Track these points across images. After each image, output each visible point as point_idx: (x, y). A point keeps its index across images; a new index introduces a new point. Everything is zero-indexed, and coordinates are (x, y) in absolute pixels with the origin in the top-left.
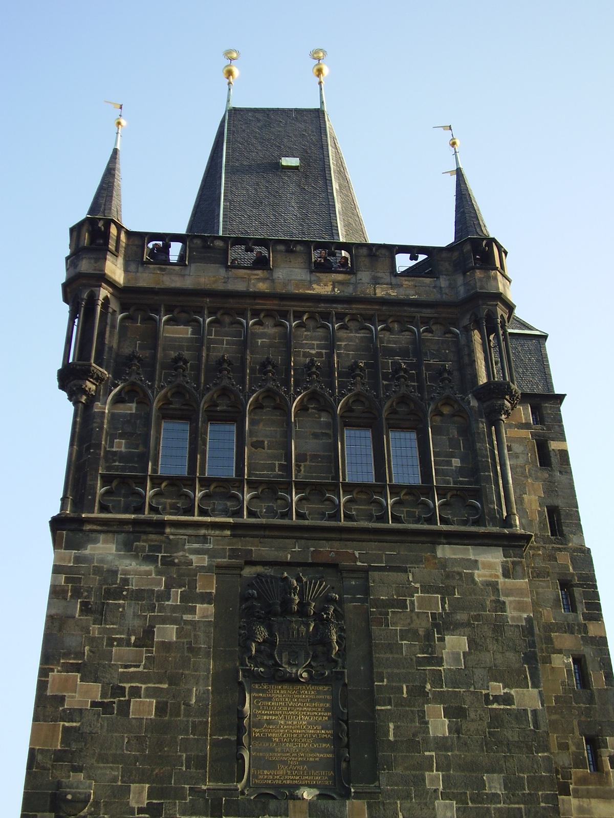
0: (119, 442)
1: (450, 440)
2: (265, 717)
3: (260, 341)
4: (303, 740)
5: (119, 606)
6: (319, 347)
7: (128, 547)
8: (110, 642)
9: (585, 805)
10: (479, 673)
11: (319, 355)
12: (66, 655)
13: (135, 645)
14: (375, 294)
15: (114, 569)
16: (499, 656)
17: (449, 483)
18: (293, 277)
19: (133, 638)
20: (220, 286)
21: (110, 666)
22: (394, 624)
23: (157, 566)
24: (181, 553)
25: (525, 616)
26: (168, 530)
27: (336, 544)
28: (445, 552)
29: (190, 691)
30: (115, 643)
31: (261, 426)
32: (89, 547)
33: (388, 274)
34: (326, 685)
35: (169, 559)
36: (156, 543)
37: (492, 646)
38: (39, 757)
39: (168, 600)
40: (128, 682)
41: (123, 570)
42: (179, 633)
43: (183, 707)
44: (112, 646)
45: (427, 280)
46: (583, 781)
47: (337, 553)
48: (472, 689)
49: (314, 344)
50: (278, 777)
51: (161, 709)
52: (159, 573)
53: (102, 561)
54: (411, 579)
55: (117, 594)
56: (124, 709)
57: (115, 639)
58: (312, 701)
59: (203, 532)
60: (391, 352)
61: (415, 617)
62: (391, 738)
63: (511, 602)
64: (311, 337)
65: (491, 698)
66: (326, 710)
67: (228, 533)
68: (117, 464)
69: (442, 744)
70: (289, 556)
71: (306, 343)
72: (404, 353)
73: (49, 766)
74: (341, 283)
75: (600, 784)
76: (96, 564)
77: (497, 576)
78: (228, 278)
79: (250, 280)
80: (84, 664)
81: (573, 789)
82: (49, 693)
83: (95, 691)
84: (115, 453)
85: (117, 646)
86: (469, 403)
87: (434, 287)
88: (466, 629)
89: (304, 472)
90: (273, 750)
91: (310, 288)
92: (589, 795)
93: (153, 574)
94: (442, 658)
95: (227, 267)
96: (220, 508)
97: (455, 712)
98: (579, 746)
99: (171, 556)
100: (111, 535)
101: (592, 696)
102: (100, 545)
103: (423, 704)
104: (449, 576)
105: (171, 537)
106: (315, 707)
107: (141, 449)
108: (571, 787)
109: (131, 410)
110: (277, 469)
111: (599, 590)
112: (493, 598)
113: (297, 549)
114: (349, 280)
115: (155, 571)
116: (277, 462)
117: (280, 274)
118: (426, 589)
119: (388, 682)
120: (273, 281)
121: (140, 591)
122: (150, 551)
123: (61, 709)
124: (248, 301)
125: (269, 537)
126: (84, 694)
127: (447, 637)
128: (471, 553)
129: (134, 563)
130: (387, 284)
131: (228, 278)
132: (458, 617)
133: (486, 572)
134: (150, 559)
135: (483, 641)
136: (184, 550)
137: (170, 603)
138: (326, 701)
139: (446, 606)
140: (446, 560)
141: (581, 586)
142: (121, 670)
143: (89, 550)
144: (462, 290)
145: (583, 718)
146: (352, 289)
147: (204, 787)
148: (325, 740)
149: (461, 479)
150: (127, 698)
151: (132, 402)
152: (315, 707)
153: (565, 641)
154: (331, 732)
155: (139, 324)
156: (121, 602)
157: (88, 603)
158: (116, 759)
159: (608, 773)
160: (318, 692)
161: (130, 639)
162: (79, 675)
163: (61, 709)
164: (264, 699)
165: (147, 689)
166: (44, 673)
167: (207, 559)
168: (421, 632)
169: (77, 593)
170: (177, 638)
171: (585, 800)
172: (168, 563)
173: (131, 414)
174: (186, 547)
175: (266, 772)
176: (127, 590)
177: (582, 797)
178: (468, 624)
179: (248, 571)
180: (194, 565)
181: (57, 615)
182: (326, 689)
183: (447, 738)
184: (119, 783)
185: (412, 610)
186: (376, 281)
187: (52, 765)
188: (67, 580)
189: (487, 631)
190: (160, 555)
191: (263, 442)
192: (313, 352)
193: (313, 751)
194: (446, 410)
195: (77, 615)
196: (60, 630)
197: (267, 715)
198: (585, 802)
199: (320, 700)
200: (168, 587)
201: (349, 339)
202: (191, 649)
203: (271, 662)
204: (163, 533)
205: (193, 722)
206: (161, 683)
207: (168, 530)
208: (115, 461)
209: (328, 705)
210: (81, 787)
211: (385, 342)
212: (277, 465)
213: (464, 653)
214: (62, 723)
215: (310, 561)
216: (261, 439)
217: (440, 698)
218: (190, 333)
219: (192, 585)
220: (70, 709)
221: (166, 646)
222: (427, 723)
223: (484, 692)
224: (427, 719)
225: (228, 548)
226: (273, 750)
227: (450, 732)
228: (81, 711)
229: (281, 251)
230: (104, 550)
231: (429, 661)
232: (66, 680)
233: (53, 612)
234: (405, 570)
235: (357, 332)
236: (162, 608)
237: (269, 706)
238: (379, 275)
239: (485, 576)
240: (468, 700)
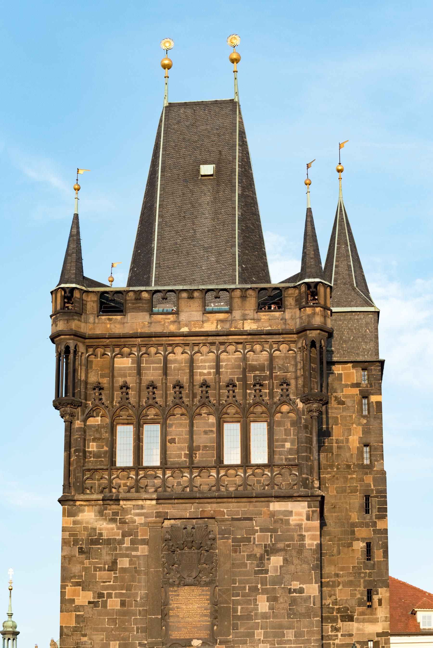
0: (92, 445)
1: (285, 429)
2: (176, 605)
3: (173, 366)
4: (195, 616)
5: (99, 548)
6: (210, 368)
7: (101, 513)
8: (95, 570)
9: (361, 627)
10: (287, 577)
11: (209, 373)
12: (74, 577)
13: (108, 571)
14: (243, 329)
15: (94, 527)
16: (299, 567)
17: (282, 460)
18: (192, 319)
19: (107, 566)
20: (147, 330)
21: (96, 582)
22: (244, 552)
23: (117, 525)
24: (129, 516)
25: (315, 543)
26: (121, 502)
27: (215, 505)
28: (276, 506)
29: (138, 593)
30: (98, 570)
31: (174, 428)
32: (80, 515)
33: (252, 311)
34: (207, 586)
35: (123, 520)
36: (116, 511)
37: (296, 561)
38: (65, 630)
39: (124, 544)
40: (106, 590)
41: (99, 528)
42: (130, 561)
43: (134, 602)
44: (96, 571)
45: (277, 314)
46: (362, 614)
47: (214, 511)
48: (283, 586)
49: (206, 366)
50: (182, 635)
51: (123, 604)
52: (118, 528)
53: (87, 523)
54: (254, 524)
55: (96, 542)
56: (105, 605)
57: (98, 567)
58: (200, 595)
59: (140, 503)
60: (253, 368)
61: (255, 548)
62: (239, 614)
63: (308, 536)
64: (204, 361)
65: (292, 590)
66: (207, 600)
67: (154, 502)
68: (92, 459)
69: (265, 616)
70: (188, 514)
71: (201, 365)
72: (262, 368)
73: (70, 634)
74: (222, 321)
75: (371, 615)
76: (84, 525)
77: (302, 520)
78: (151, 323)
79: (165, 323)
80: (83, 582)
81: (356, 618)
82: (67, 598)
83: (90, 596)
84: (90, 452)
85: (99, 571)
86: (297, 405)
87: (281, 319)
88: (282, 552)
89: (199, 458)
90: (179, 622)
91: (202, 327)
92: (364, 621)
93: (115, 529)
94: (268, 570)
95: (152, 313)
96: (151, 484)
97: (273, 599)
98: (362, 594)
99: (124, 518)
100: (91, 507)
101: (374, 565)
102: (86, 513)
103: (257, 595)
104: (276, 522)
105: (124, 506)
106: (201, 598)
107: (106, 448)
108: (355, 617)
109: (98, 422)
110: (183, 457)
111: (388, 499)
112: (299, 533)
113: (192, 510)
114: (227, 318)
115: (116, 528)
116: (183, 453)
117: (183, 317)
118: (262, 530)
119: (239, 584)
120: (179, 322)
121: (109, 540)
122: (113, 515)
123: (74, 605)
124: (164, 338)
125: (177, 503)
126: (83, 598)
127: (272, 558)
128: (289, 506)
129: (105, 524)
130: (251, 320)
131: (151, 323)
132: (279, 546)
133: (297, 518)
134: (113, 520)
135: (291, 558)
136: (131, 514)
137: (125, 545)
138: (207, 595)
139: (273, 539)
140: (275, 512)
141: (377, 497)
142: (102, 584)
143: (81, 517)
144: (298, 321)
145: (367, 578)
146: (228, 325)
147: (146, 642)
148: (206, 616)
149: (290, 456)
150: (105, 599)
151: (97, 415)
152: (201, 598)
153: (363, 532)
154: (209, 611)
155: (99, 359)
156: (99, 546)
157: (82, 548)
158: (103, 630)
159: (376, 609)
160: (203, 591)
161: (105, 567)
162: (81, 587)
163: (74, 605)
164: (175, 595)
165: (115, 593)
166: (63, 587)
167: (143, 519)
168: (258, 555)
169: (76, 542)
170: (130, 565)
171: (361, 623)
172: (123, 522)
173: (98, 425)
174: (132, 512)
175: (176, 633)
176: (102, 539)
177: (360, 622)
178: (284, 550)
179: (167, 523)
180: (137, 522)
181: (67, 555)
182: (207, 588)
183: (267, 612)
184: (105, 641)
185: (254, 543)
186: (244, 318)
187: (72, 634)
188: (70, 535)
189: (294, 553)
190: (118, 518)
191: (175, 439)
192: (205, 371)
193: (199, 621)
194: (285, 408)
195: (77, 554)
196: (69, 564)
197: (177, 604)
198: (361, 625)
199: (203, 595)
200: (124, 536)
201: (228, 360)
202: (136, 571)
203: (178, 575)
204: (119, 504)
205: (139, 610)
206: (122, 590)
207: (121, 502)
208: (91, 458)
209: (208, 597)
210: (87, 644)
211: (250, 361)
212: (183, 454)
213: (280, 566)
214: (74, 613)
215: (199, 517)
216: (173, 437)
217: (265, 591)
218: (130, 363)
219: (136, 535)
220: (78, 605)
221: (123, 570)
222: (258, 605)
223: (289, 587)
224: (258, 603)
225: (155, 511)
226: (179, 622)
227: (269, 610)
228: (83, 606)
229: (184, 298)
230: (88, 516)
231: (261, 572)
232: (75, 590)
233: (65, 554)
234: (251, 519)
235: (233, 355)
236: (121, 549)
237: (177, 599)
238: (247, 312)
239: (296, 520)
240: (280, 592)
